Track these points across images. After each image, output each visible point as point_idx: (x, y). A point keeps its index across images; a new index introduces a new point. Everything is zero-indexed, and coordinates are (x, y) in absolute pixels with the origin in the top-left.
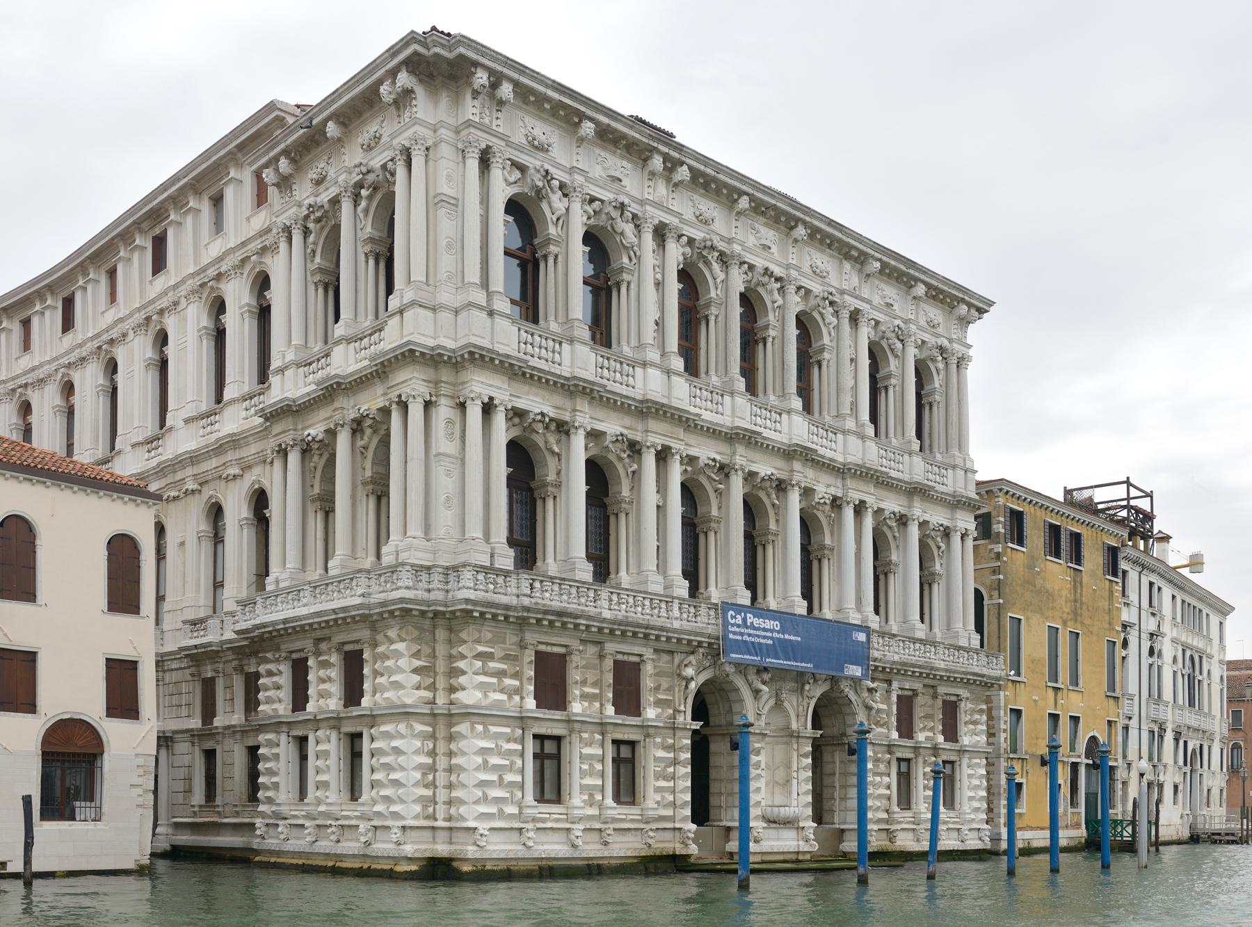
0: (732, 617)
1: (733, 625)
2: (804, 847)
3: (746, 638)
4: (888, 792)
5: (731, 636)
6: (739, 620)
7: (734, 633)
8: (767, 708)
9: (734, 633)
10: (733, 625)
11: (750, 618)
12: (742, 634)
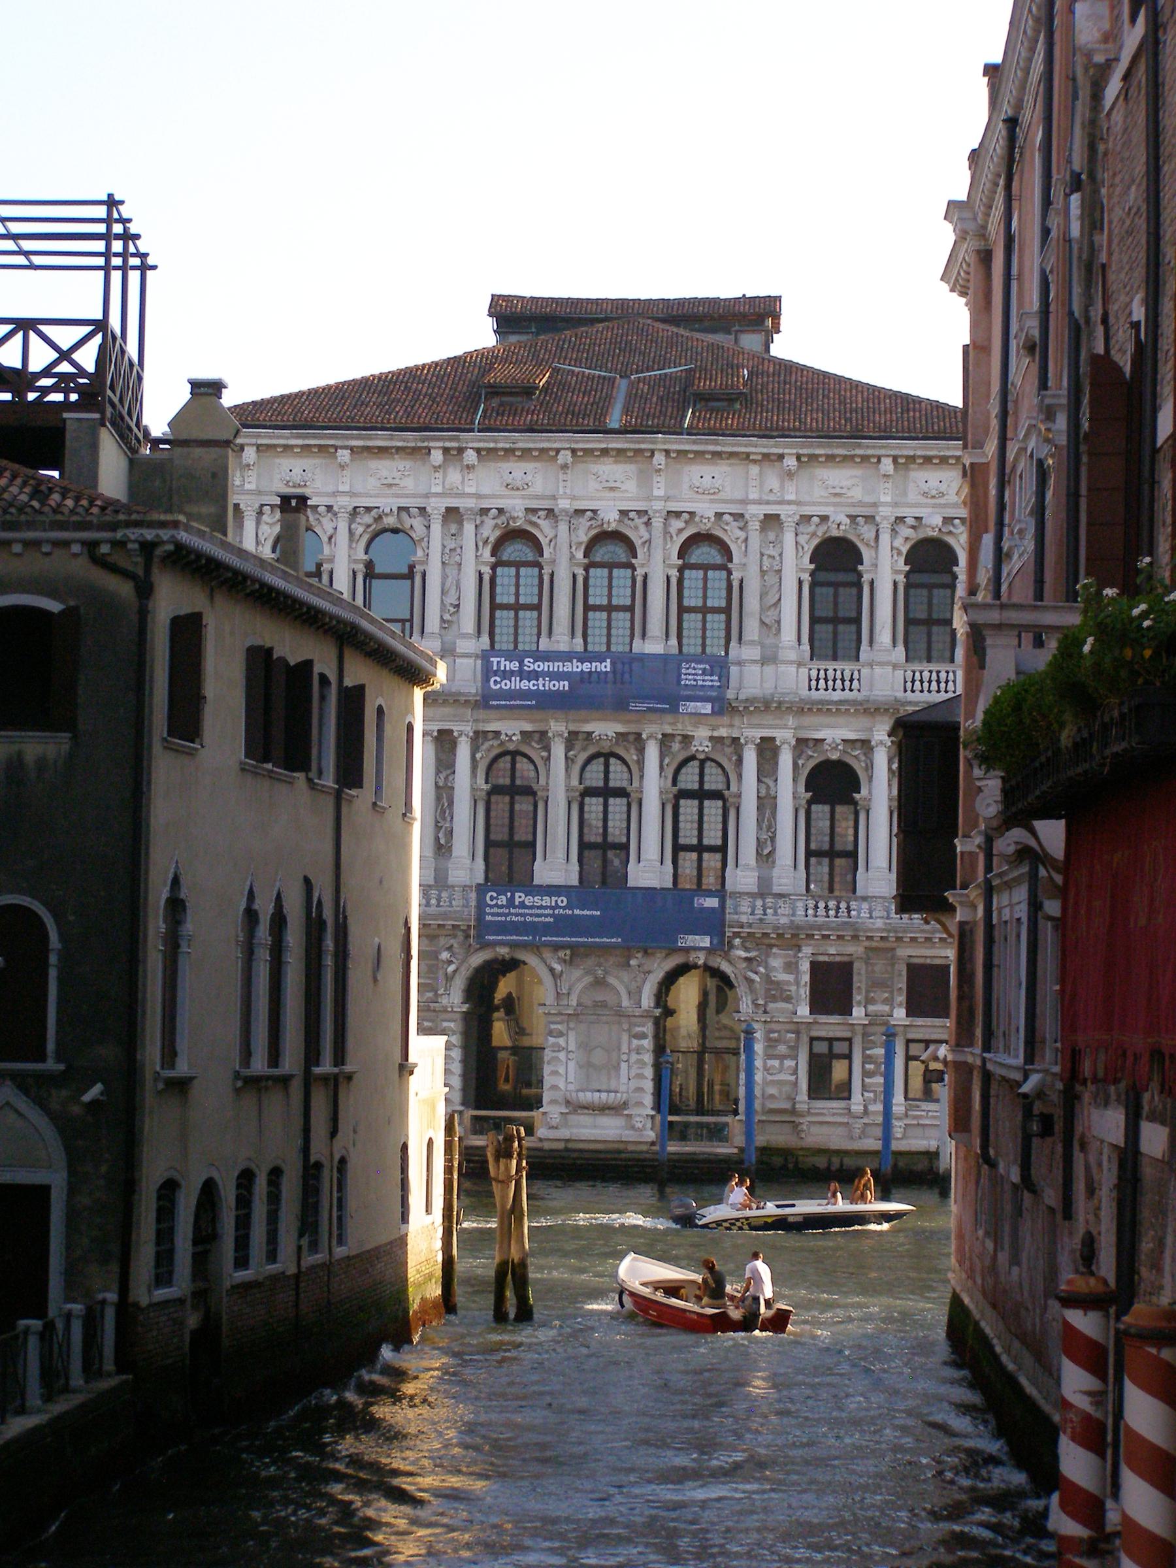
0: (492, 898)
1: (492, 907)
2: (629, 1135)
3: (529, 919)
4: (793, 1078)
5: (488, 918)
6: (503, 900)
7: (493, 915)
8: (579, 986)
9: (493, 915)
10: (492, 907)
11: (519, 897)
12: (506, 915)
